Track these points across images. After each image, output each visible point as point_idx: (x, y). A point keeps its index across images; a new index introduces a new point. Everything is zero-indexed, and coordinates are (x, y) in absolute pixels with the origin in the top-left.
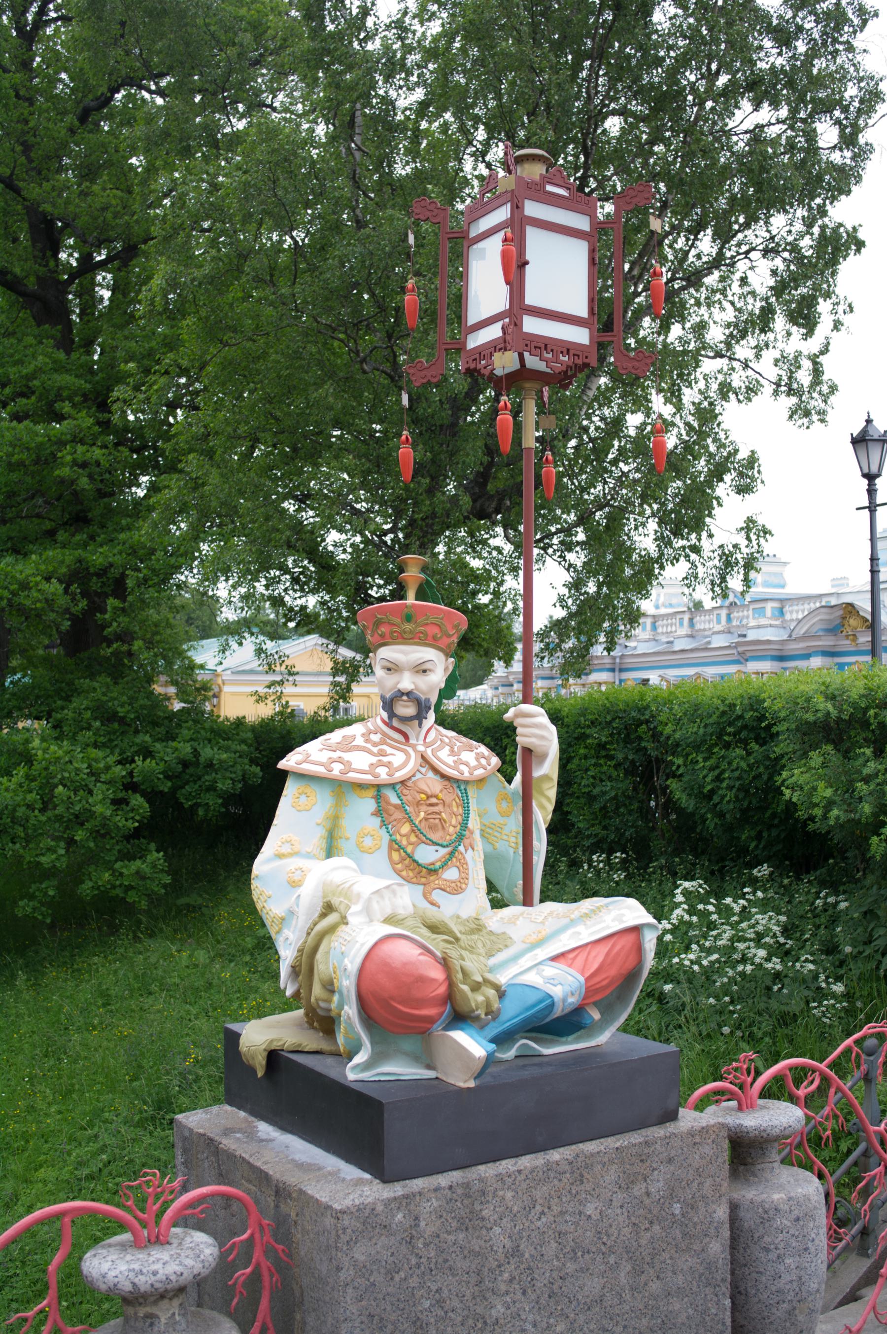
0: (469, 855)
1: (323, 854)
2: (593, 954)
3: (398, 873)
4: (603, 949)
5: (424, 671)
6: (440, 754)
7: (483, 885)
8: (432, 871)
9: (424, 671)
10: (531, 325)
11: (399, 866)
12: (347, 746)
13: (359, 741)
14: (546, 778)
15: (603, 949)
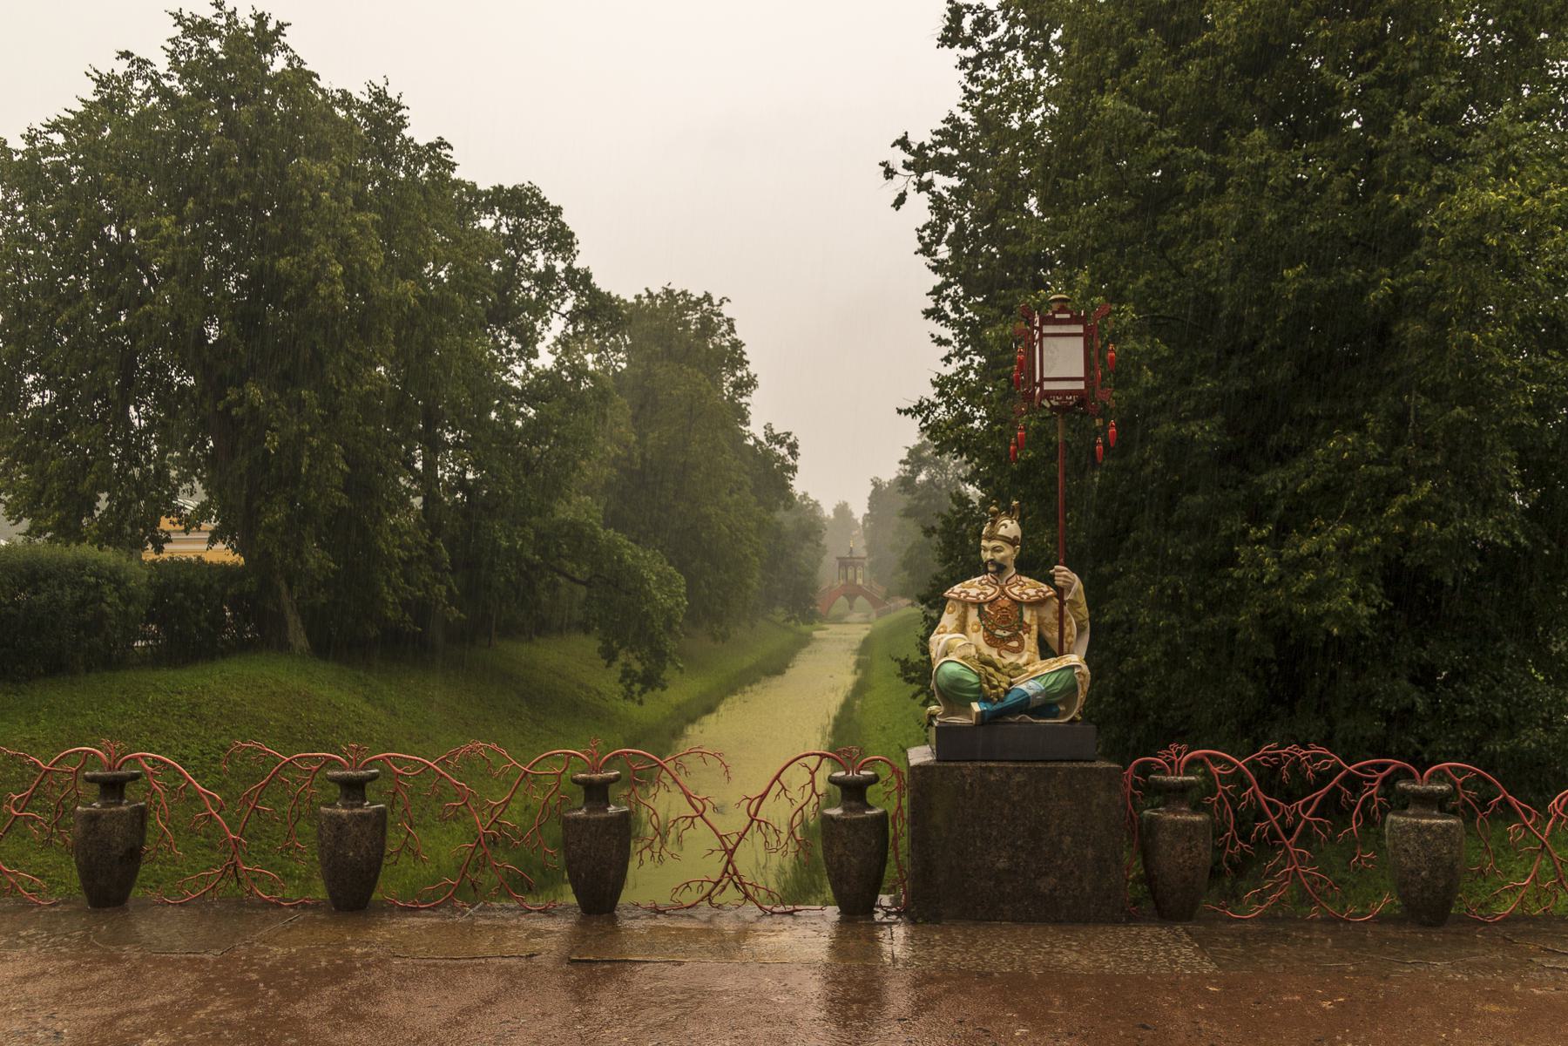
0: (1026, 637)
3: (986, 641)
4: (1056, 675)
8: (1003, 639)
10: (1048, 386)
12: (971, 586)
13: (976, 584)
15: (1056, 675)
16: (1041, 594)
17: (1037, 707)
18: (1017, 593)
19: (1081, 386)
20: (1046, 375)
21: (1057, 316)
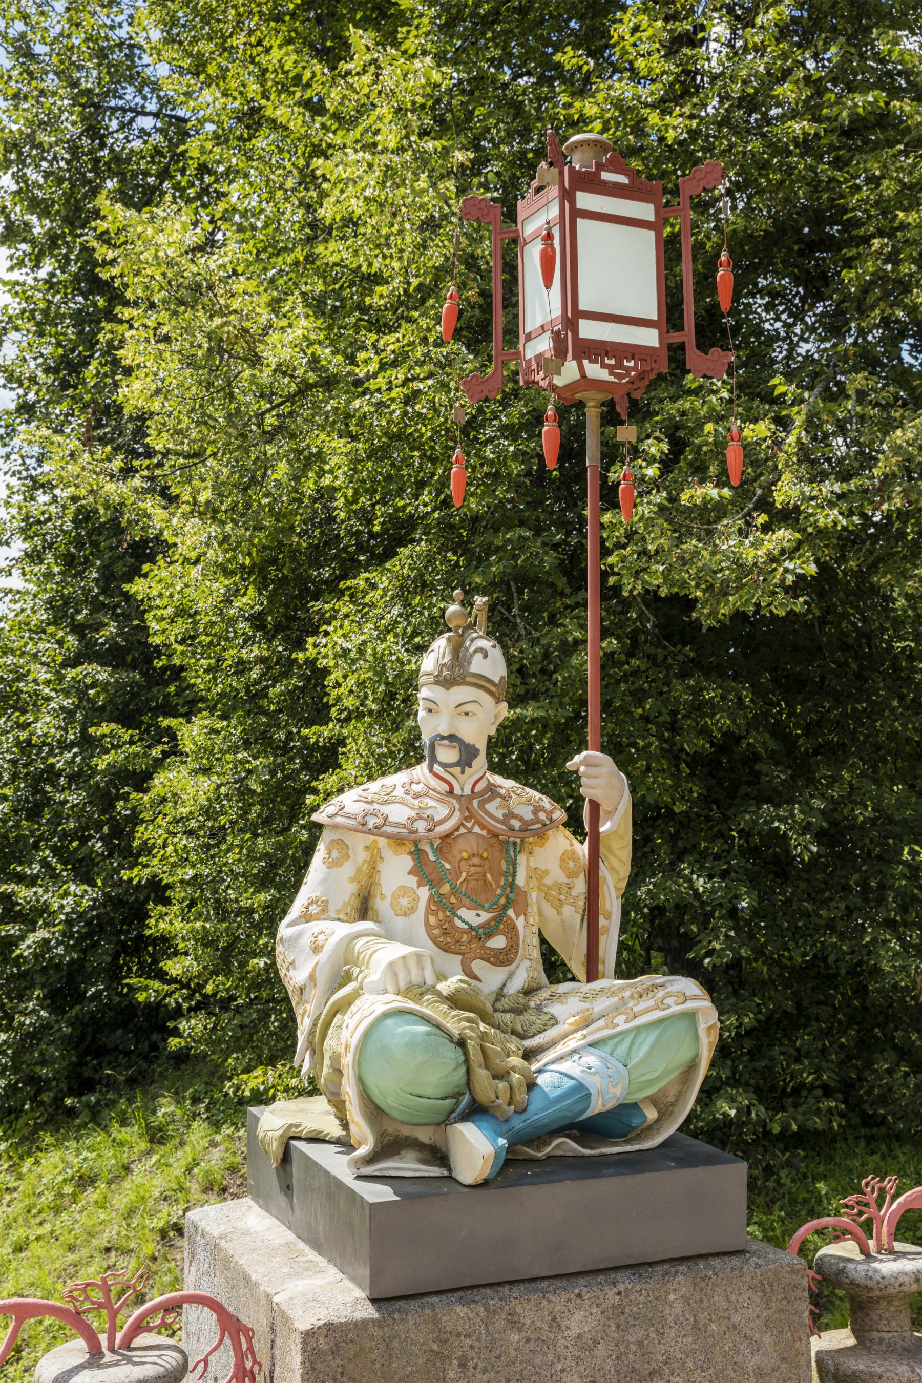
1: (354, 914)
2: (640, 1040)
5: (467, 714)
6: (487, 806)
7: (536, 953)
9: (467, 714)
11: (436, 931)
13: (399, 792)
14: (612, 833)
16: (542, 816)
17: (600, 1115)
18: (499, 814)
19: (650, 338)
20: (582, 306)
21: (606, 176)
